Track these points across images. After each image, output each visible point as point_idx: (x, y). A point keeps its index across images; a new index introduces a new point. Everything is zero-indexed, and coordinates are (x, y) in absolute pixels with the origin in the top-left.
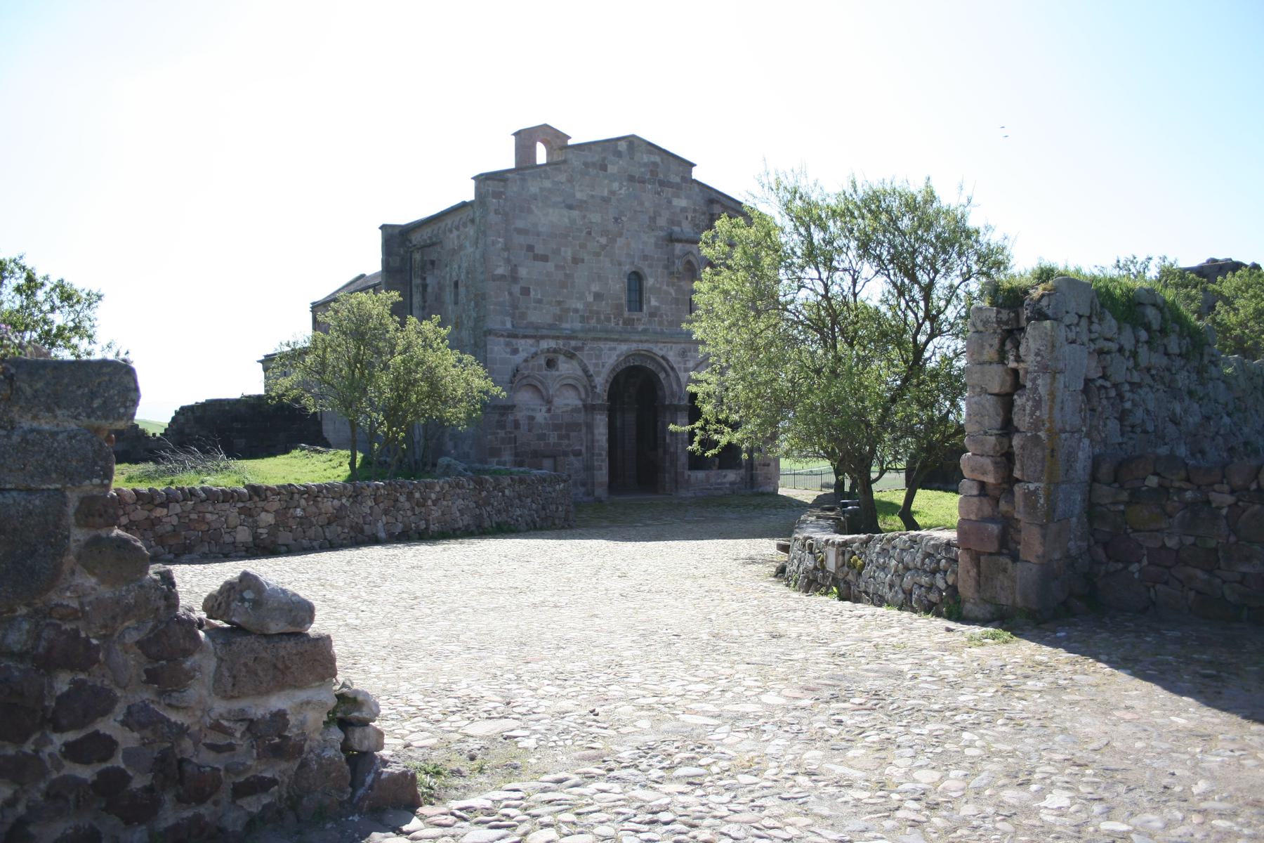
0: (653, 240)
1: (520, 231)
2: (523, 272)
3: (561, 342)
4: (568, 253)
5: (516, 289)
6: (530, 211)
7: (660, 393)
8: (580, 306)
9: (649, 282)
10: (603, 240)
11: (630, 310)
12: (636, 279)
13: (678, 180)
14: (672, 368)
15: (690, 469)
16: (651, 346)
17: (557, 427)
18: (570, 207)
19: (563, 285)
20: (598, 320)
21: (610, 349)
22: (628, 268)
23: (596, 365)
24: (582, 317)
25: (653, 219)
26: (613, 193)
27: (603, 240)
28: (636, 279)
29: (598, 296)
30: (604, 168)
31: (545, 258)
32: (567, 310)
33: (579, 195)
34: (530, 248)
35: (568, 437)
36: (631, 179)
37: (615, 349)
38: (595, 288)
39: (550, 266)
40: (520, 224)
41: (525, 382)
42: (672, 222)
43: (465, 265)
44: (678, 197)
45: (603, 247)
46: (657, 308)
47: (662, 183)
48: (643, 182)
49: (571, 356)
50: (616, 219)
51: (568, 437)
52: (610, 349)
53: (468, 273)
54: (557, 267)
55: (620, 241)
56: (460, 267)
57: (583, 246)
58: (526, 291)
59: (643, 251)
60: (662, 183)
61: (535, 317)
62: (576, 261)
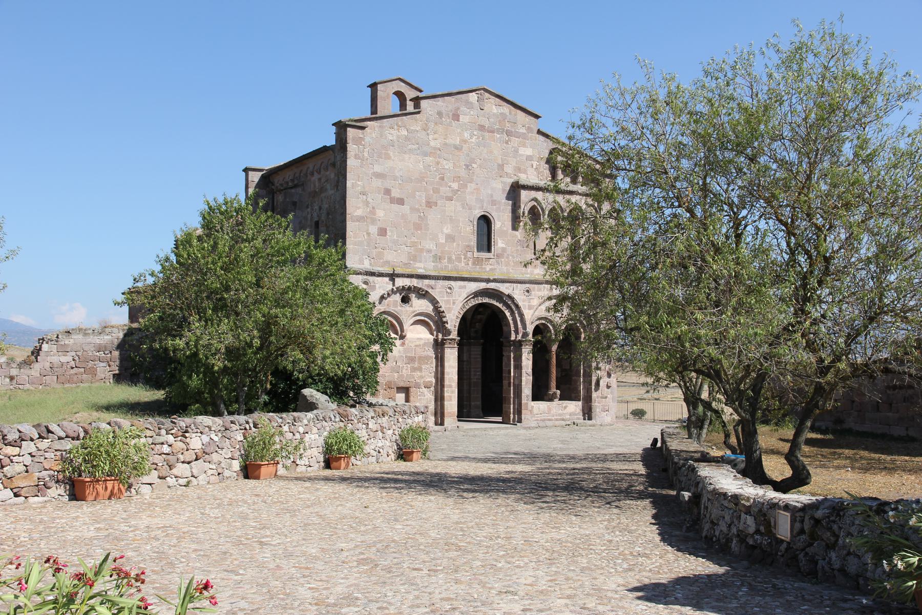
0: (500, 186)
1: (379, 176)
2: (380, 213)
4: (421, 197)
5: (373, 230)
6: (388, 157)
7: (505, 328)
8: (432, 246)
9: (497, 226)
10: (455, 186)
11: (478, 250)
12: (485, 222)
13: (523, 130)
14: (517, 306)
15: (533, 400)
16: (498, 284)
17: (411, 360)
18: (425, 154)
19: (418, 227)
20: (450, 259)
21: (461, 287)
22: (478, 213)
23: (448, 302)
24: (435, 256)
25: (501, 167)
26: (465, 141)
27: (455, 186)
28: (485, 222)
29: (450, 238)
30: (456, 117)
32: (421, 250)
33: (432, 144)
34: (387, 192)
35: (420, 369)
36: (482, 128)
37: (465, 287)
38: (447, 230)
39: (406, 209)
40: (377, 169)
42: (519, 169)
43: (326, 206)
44: (524, 146)
45: (455, 192)
46: (504, 250)
47: (509, 133)
48: (493, 132)
49: (423, 294)
50: (467, 166)
51: (420, 369)
52: (461, 287)
53: (328, 214)
54: (413, 209)
55: (471, 187)
56: (320, 208)
57: (436, 191)
58: (383, 232)
59: (492, 196)
60: (509, 133)
61: (390, 256)
62: (429, 204)
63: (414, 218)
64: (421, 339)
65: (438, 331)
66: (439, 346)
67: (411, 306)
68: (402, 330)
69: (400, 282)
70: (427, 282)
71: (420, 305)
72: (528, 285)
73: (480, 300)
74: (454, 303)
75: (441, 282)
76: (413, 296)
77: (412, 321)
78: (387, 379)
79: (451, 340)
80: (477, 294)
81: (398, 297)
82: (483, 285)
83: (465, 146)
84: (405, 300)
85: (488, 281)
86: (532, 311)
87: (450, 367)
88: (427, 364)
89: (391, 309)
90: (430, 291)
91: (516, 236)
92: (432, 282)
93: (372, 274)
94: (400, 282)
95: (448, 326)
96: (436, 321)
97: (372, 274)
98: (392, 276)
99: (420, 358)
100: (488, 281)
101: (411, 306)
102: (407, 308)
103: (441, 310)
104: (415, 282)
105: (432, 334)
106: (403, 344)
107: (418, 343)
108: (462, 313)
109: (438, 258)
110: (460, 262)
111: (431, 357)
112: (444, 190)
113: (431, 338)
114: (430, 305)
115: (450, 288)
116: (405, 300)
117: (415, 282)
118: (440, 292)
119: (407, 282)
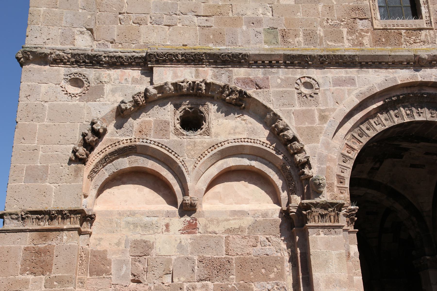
21: (338, 82)
23: (305, 115)
37: (352, 81)
41: (125, 163)
49: (237, 103)
52: (338, 82)
64: (243, 213)
65: (291, 192)
66: (294, 226)
67: (208, 133)
68: (185, 192)
69: (165, 75)
70: (240, 72)
71: (225, 128)
73: (403, 116)
74: (323, 118)
75: (281, 74)
76: (211, 111)
77: (214, 171)
79: (326, 206)
80: (392, 99)
81: (169, 114)
82: (403, 76)
84: (192, 122)
85: (417, 63)
87: (329, 282)
88: (266, 278)
89: (153, 140)
90: (251, 92)
92: (257, 73)
93: (93, 61)
94: (165, 75)
95: (313, 172)
96: (283, 163)
97: (93, 61)
98: (146, 63)
99: (243, 263)
100: (417, 63)
101: (208, 133)
102: (196, 138)
103: (290, 134)
104: (208, 74)
105: (277, 201)
106: (191, 228)
107: (234, 224)
108: (358, 147)
110: (340, 39)
111: (280, 261)
113: (274, 210)
114: (260, 126)
115: (308, 85)
116: (192, 122)
117: (208, 74)
118: (281, 95)
119: (186, 74)
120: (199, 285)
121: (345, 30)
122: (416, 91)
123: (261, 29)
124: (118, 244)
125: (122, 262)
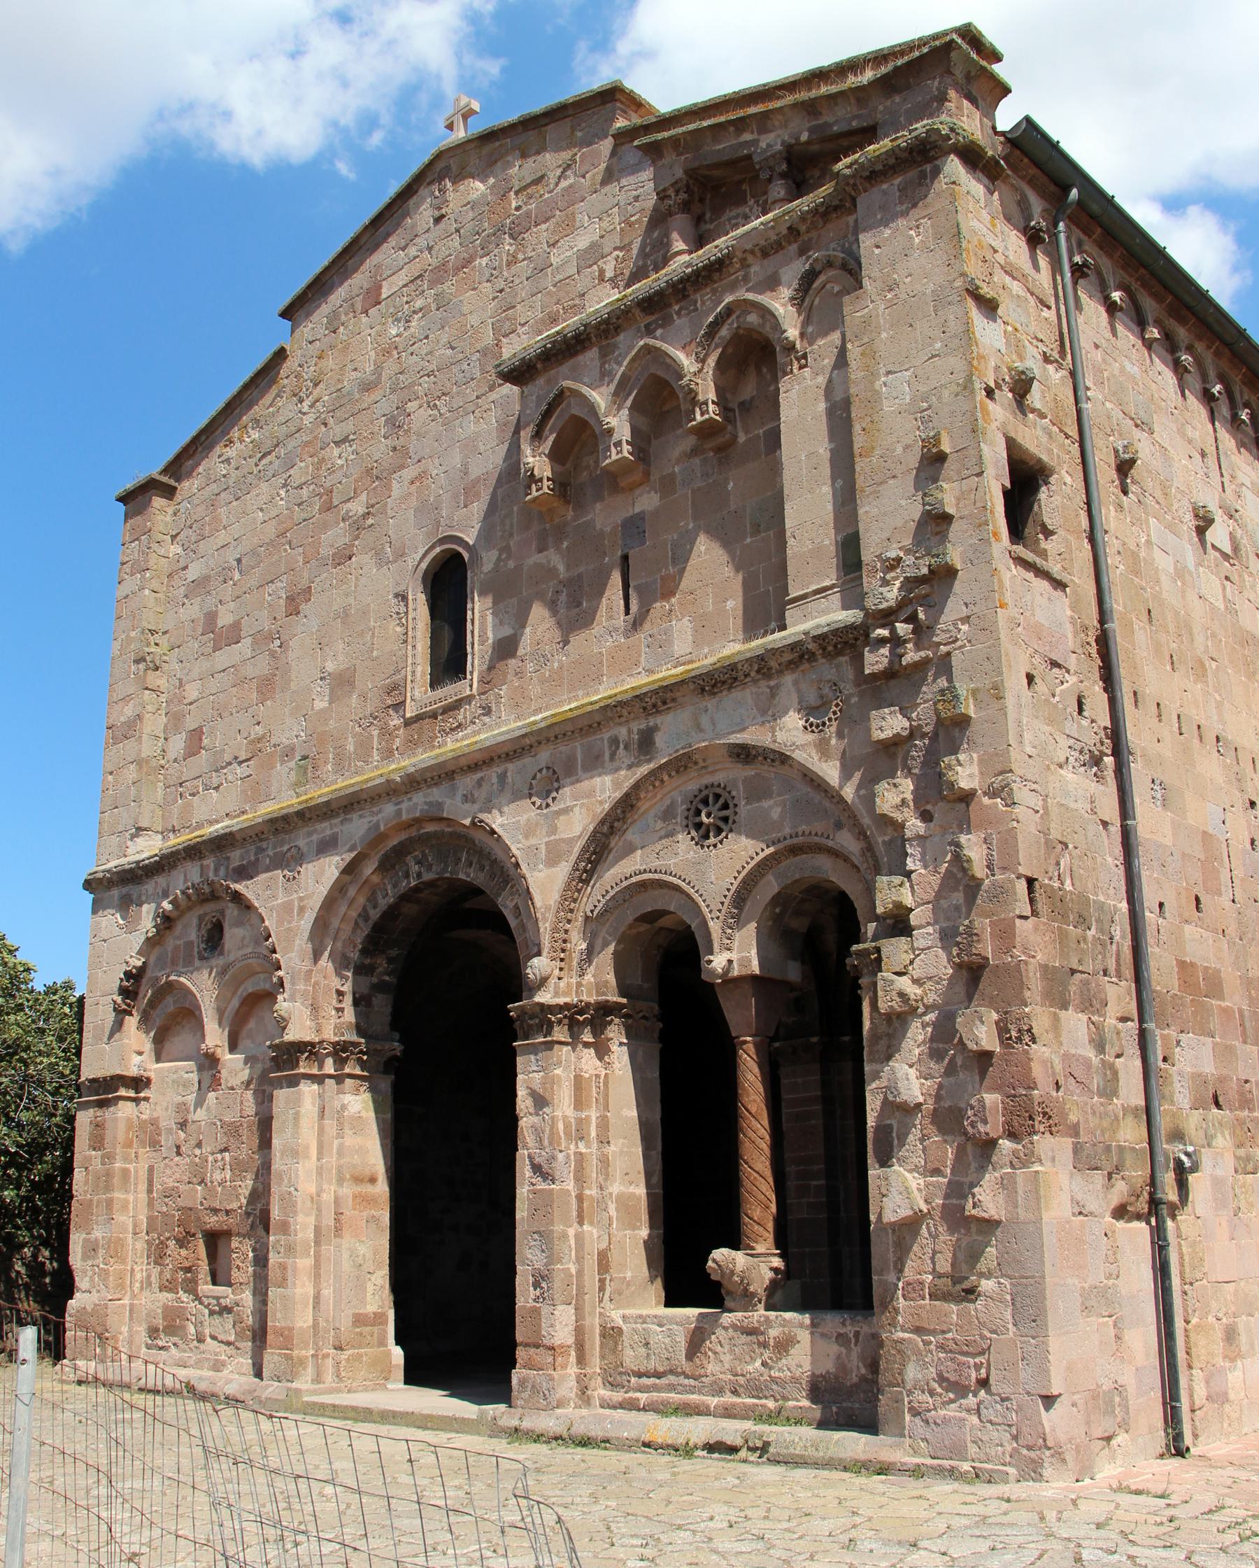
3: (209, 862)
4: (280, 588)
16: (436, 794)
23: (287, 907)
29: (342, 683)
30: (373, 297)
31: (233, 635)
36: (440, 273)
39: (245, 647)
44: (569, 226)
45: (358, 526)
48: (468, 262)
63: (261, 666)
72: (544, 756)
74: (302, 910)
78: (181, 1202)
83: (390, 367)
86: (562, 871)
91: (552, 571)
109: (308, 765)
112: (336, 536)
120: (219, 1156)
121: (376, 733)
122: (413, 832)
123: (292, 764)
124: (167, 1109)
125: (169, 1131)
